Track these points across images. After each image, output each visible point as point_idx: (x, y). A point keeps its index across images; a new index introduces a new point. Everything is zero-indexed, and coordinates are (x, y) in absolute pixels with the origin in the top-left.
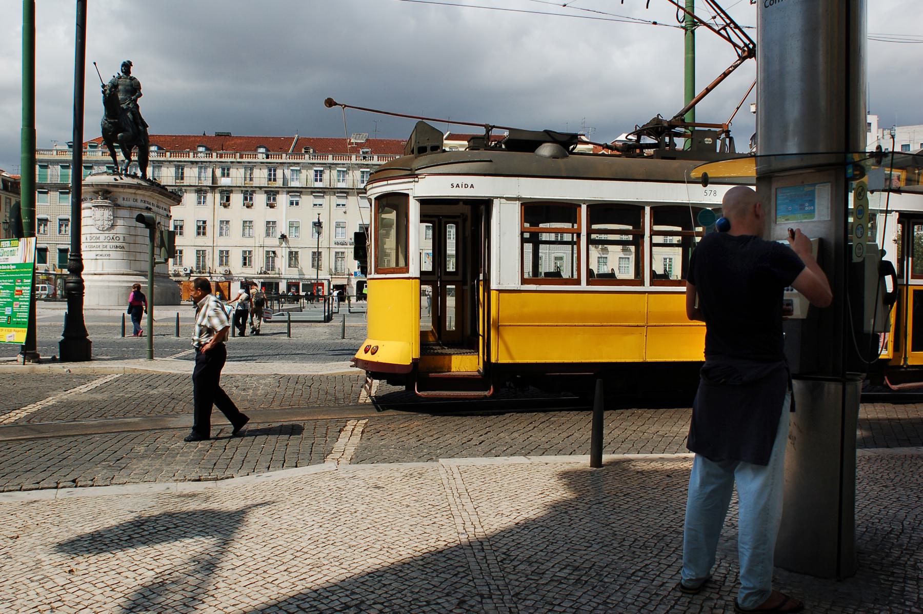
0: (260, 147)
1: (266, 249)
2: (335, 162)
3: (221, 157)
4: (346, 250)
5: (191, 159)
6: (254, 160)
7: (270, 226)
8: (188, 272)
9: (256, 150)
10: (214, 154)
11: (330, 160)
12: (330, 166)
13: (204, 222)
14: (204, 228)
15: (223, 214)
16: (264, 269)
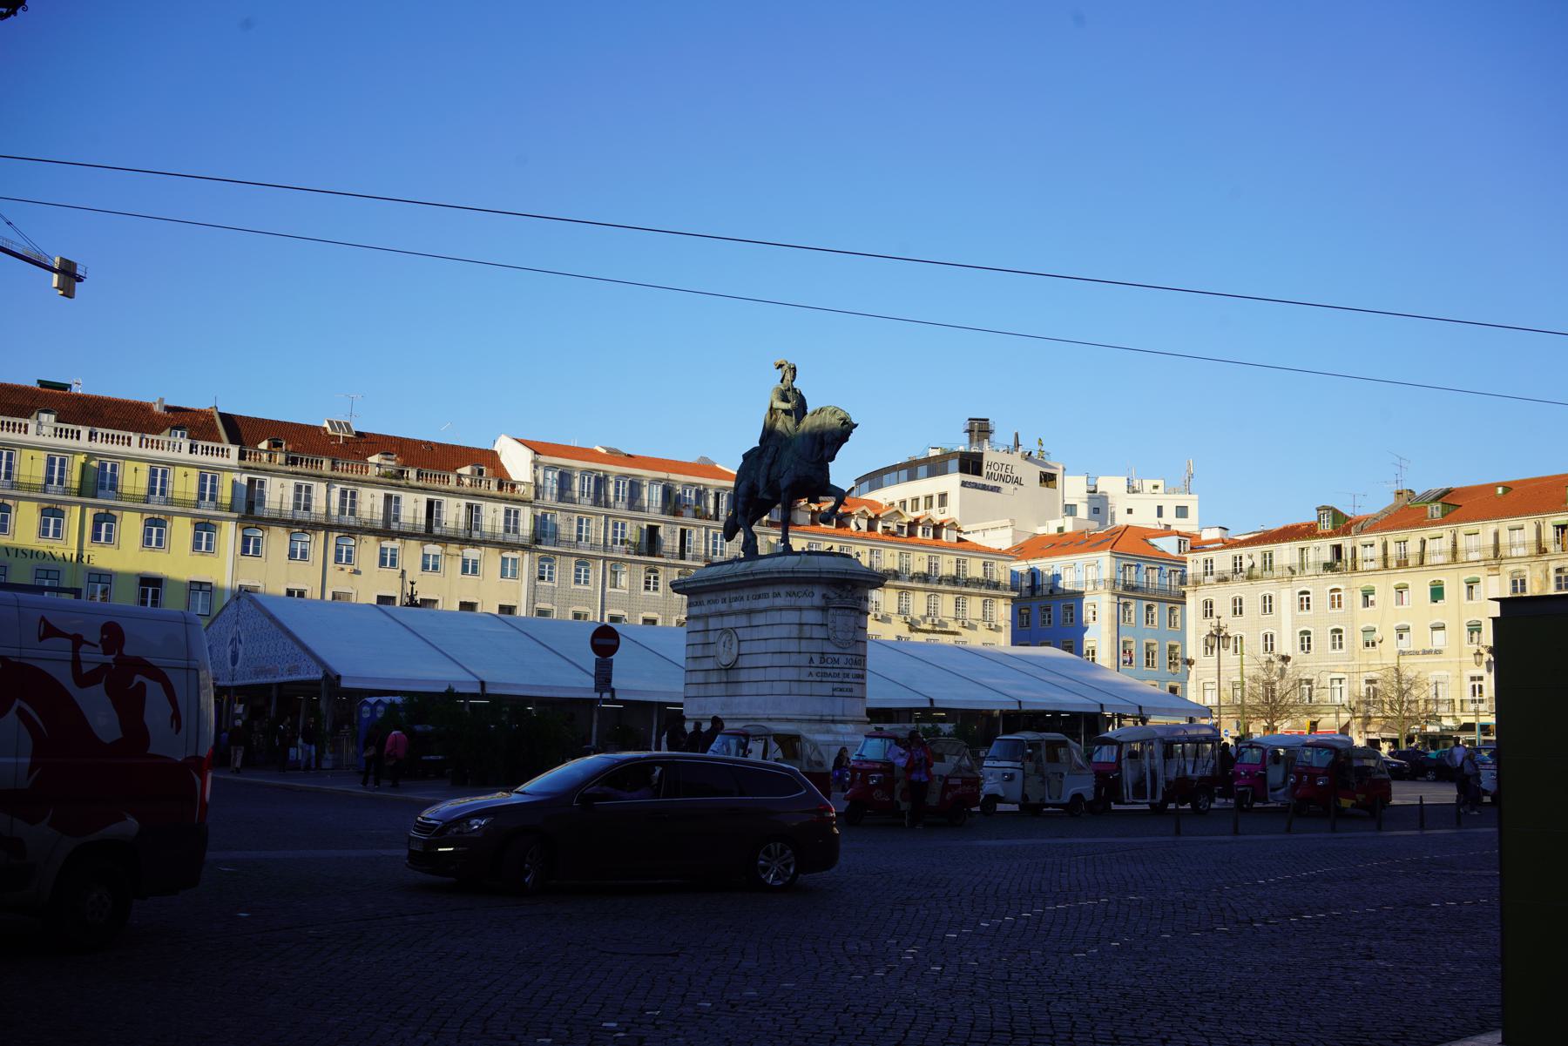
2: (335, 473)
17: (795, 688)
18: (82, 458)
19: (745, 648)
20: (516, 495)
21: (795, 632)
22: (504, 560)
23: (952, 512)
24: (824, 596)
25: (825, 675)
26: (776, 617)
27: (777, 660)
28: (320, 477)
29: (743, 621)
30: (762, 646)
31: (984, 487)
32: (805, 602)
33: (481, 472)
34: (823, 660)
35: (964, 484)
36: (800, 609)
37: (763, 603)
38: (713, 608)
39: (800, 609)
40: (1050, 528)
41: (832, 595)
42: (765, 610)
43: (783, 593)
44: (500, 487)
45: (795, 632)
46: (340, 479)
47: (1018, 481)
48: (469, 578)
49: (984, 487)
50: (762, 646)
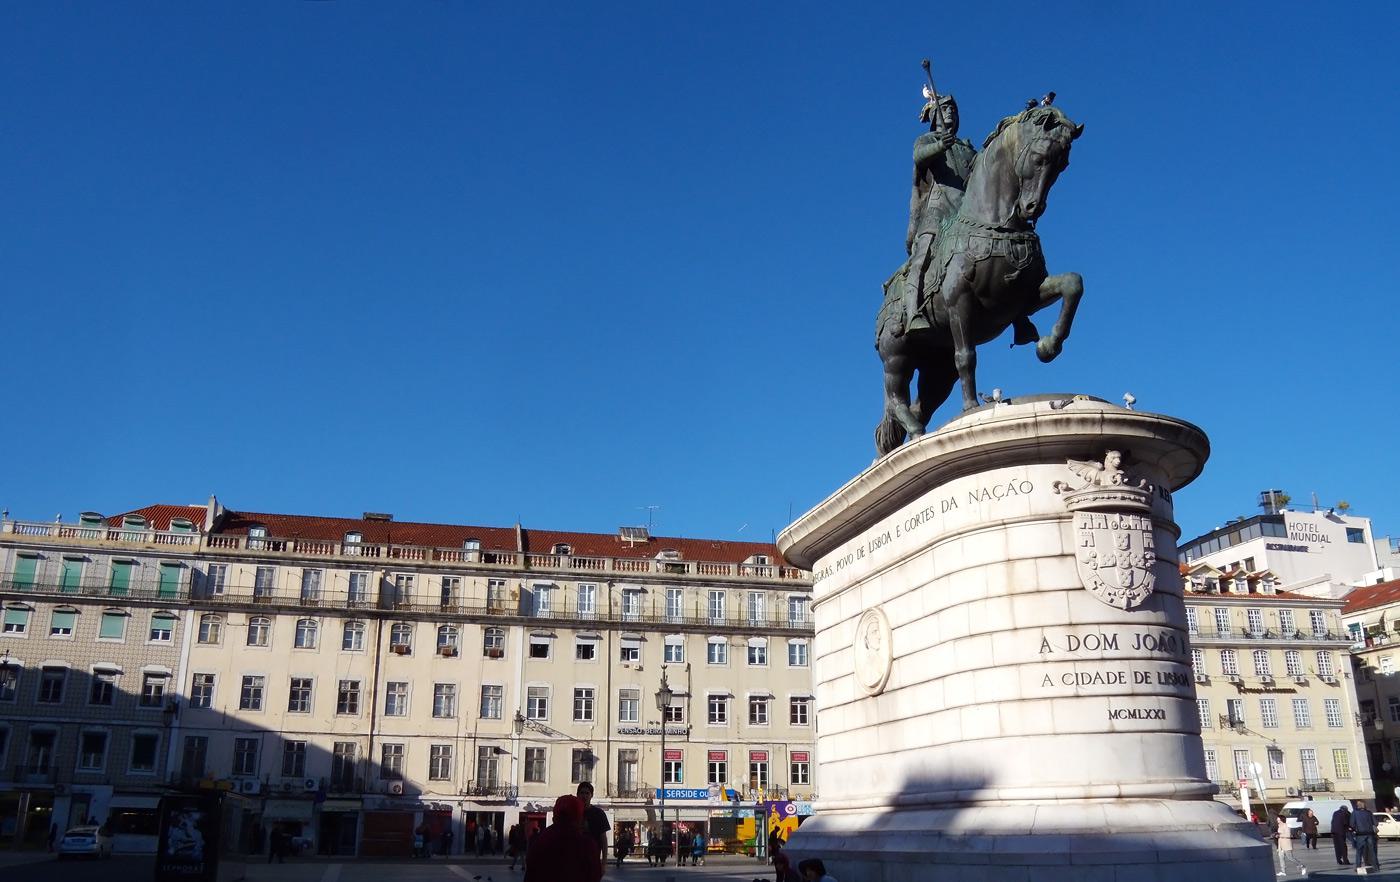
0: (470, 540)
1: (480, 743)
2: (617, 572)
3: (396, 554)
4: (639, 747)
5: (337, 556)
6: (462, 565)
7: (489, 696)
8: (316, 788)
9: (460, 545)
10: (384, 550)
11: (608, 567)
12: (612, 580)
13: (355, 685)
14: (354, 697)
15: (395, 668)
16: (474, 785)
18: (378, 575)
19: (903, 642)
20: (798, 581)
22: (792, 648)
23: (1261, 566)
25: (1079, 679)
26: (949, 556)
28: (600, 578)
31: (1290, 548)
33: (763, 561)
34: (1075, 643)
35: (1269, 547)
40: (1370, 580)
41: (1077, 483)
44: (782, 574)
46: (622, 579)
47: (1324, 539)
48: (756, 666)
49: (1290, 548)
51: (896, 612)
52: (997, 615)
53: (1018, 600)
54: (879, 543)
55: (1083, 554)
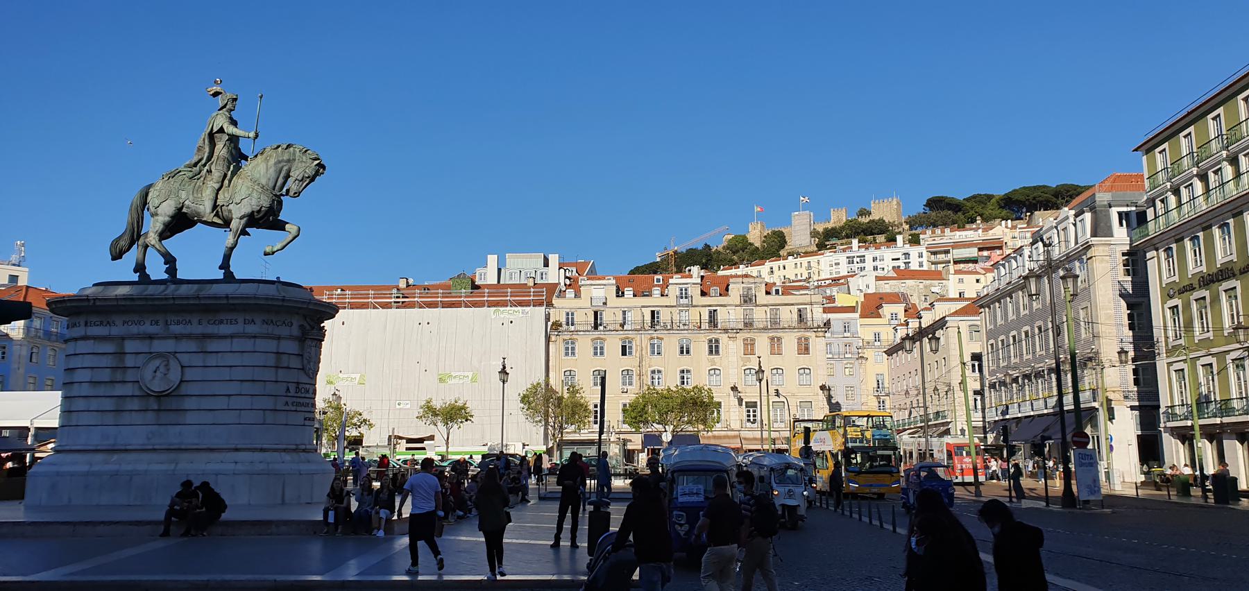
17: (270, 417)
21: (271, 360)
24: (301, 327)
27: (247, 388)
29: (192, 346)
30: (226, 374)
32: (284, 331)
34: (298, 389)
36: (279, 338)
37: (225, 329)
38: (134, 329)
39: (279, 338)
42: (232, 336)
43: (258, 321)
45: (271, 360)
50: (226, 374)
51: (185, 359)
52: (269, 375)
53: (280, 371)
54: (178, 323)
55: (306, 355)
